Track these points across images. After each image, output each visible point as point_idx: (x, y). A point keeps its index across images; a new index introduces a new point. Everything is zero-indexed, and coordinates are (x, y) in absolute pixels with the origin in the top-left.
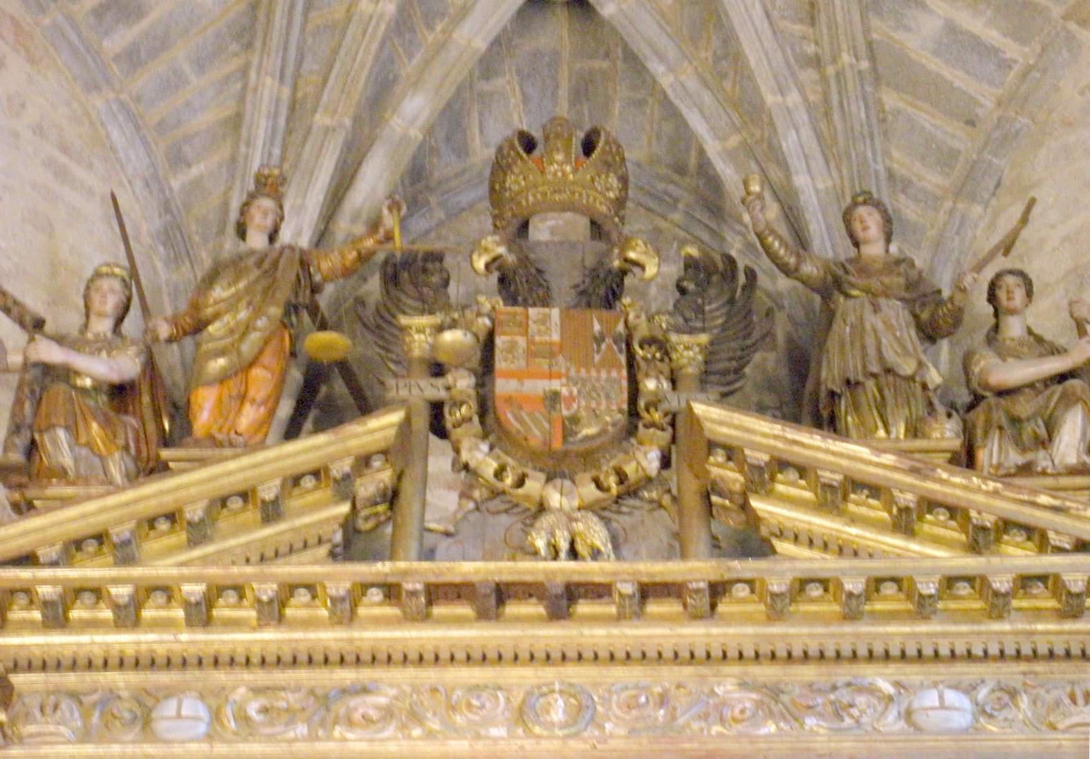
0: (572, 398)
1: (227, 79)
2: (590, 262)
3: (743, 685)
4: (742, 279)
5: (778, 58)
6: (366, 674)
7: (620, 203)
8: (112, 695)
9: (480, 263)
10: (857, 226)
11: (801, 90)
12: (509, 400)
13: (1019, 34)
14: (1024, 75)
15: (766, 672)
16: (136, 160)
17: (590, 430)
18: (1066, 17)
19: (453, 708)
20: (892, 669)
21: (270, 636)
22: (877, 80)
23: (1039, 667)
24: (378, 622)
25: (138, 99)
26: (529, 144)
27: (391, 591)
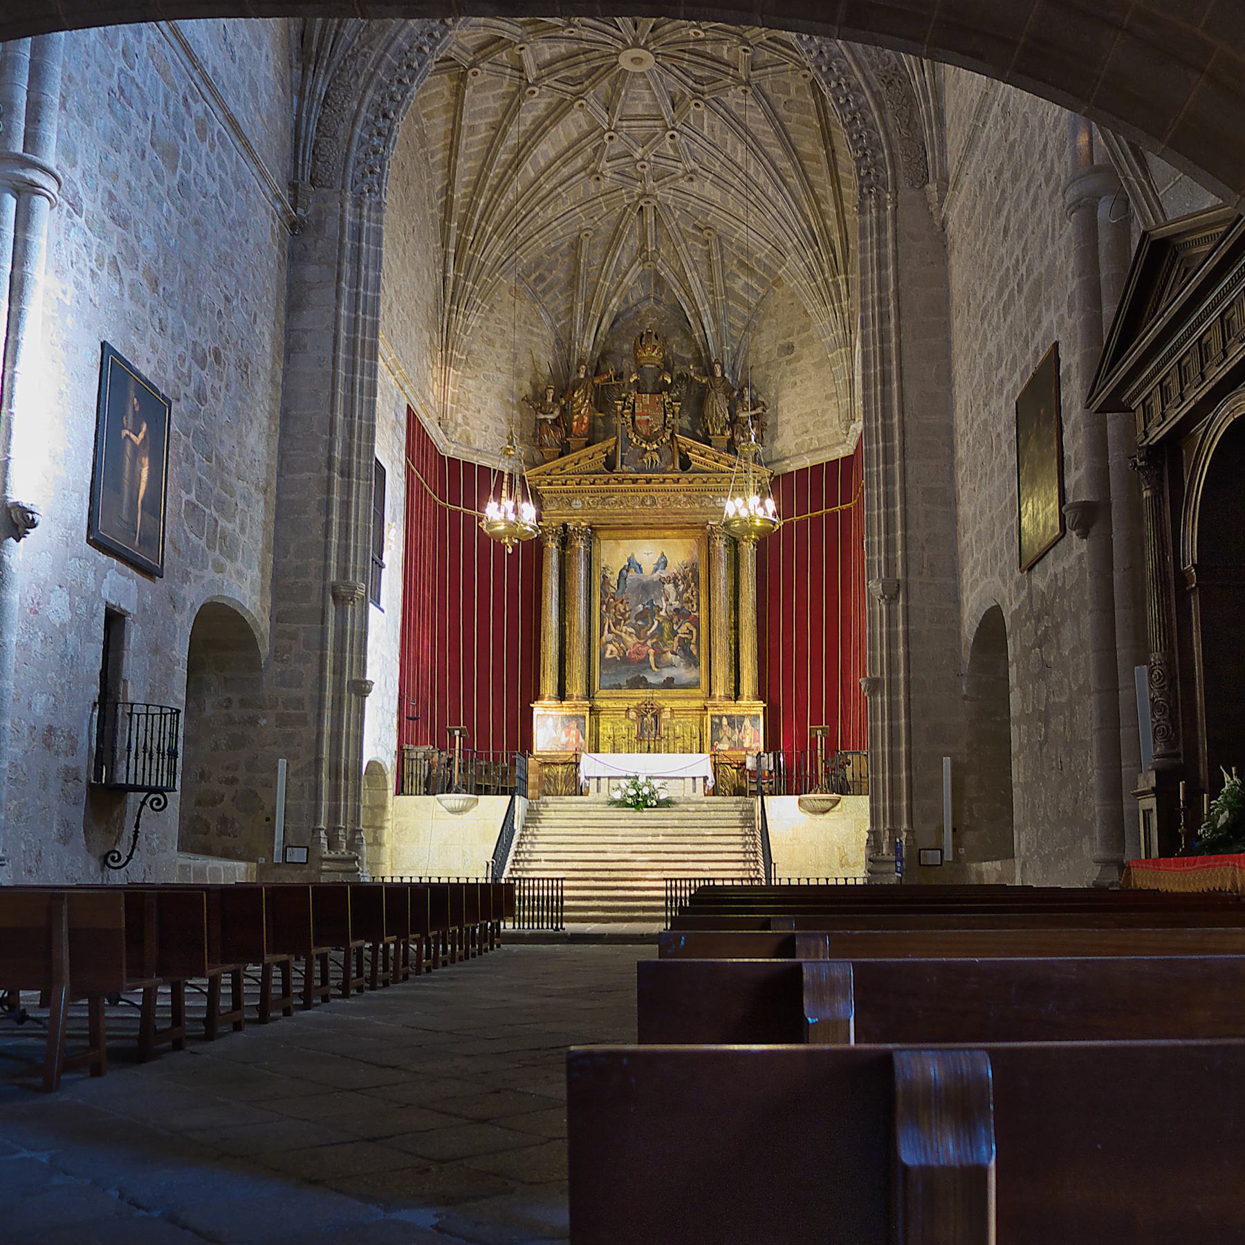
1: (568, 296)
9: (632, 380)
15: (688, 493)
16: (547, 321)
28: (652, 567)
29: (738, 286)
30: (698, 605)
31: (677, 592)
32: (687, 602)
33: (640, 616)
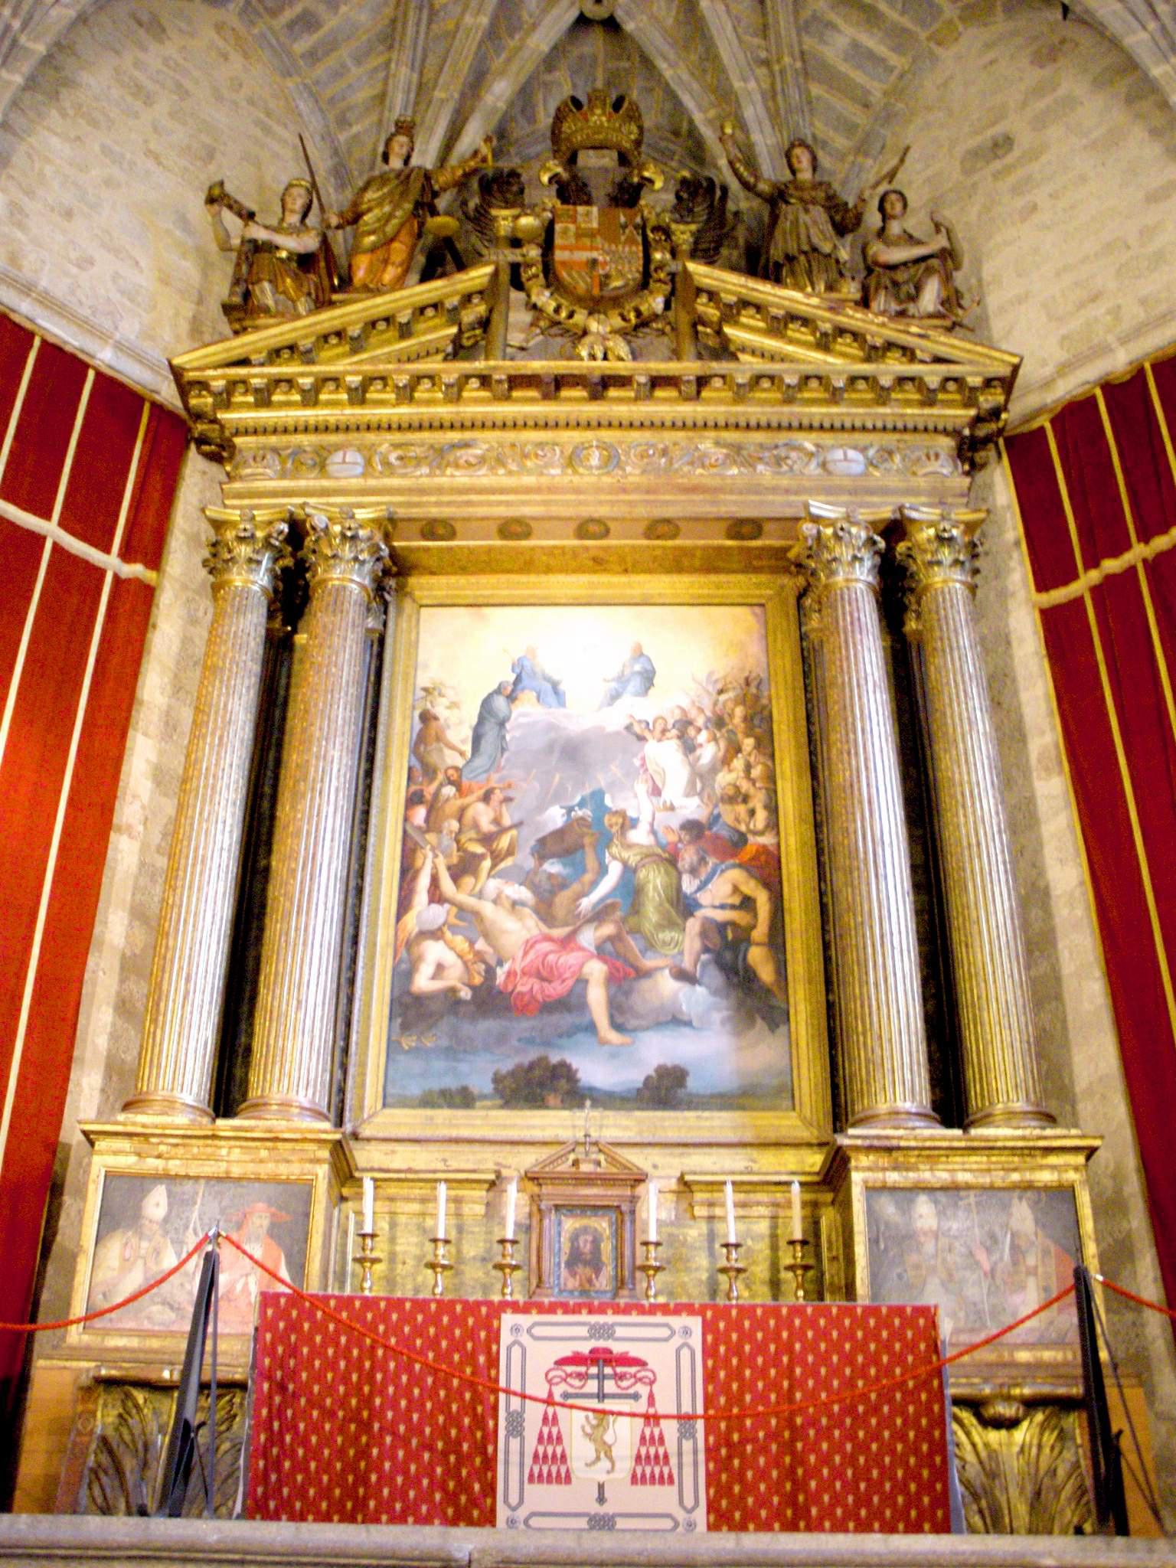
0: (605, 263)
1: (375, 70)
2: (618, 179)
3: (717, 444)
4: (718, 193)
5: (742, 61)
6: (468, 435)
7: (638, 143)
8: (299, 451)
9: (545, 179)
10: (794, 161)
11: (757, 80)
12: (564, 263)
13: (898, 49)
14: (901, 77)
16: (314, 124)
17: (617, 283)
18: (929, 39)
19: (526, 456)
20: (814, 435)
21: (405, 411)
22: (806, 74)
23: (907, 437)
24: (477, 401)
25: (317, 83)
26: (576, 103)
27: (485, 380)
28: (604, 689)
29: (833, 49)
30: (773, 809)
31: (693, 766)
32: (731, 800)
33: (552, 845)
